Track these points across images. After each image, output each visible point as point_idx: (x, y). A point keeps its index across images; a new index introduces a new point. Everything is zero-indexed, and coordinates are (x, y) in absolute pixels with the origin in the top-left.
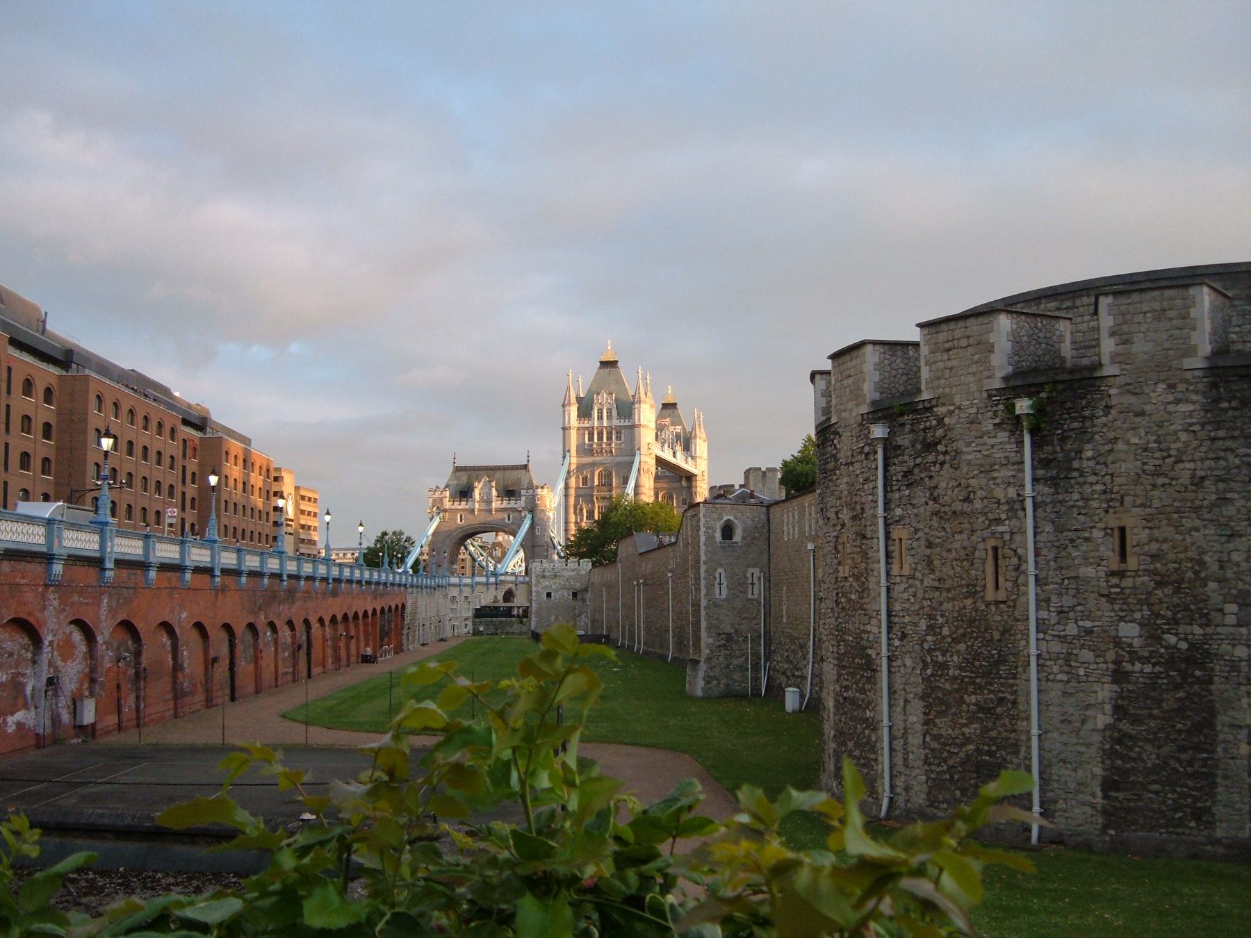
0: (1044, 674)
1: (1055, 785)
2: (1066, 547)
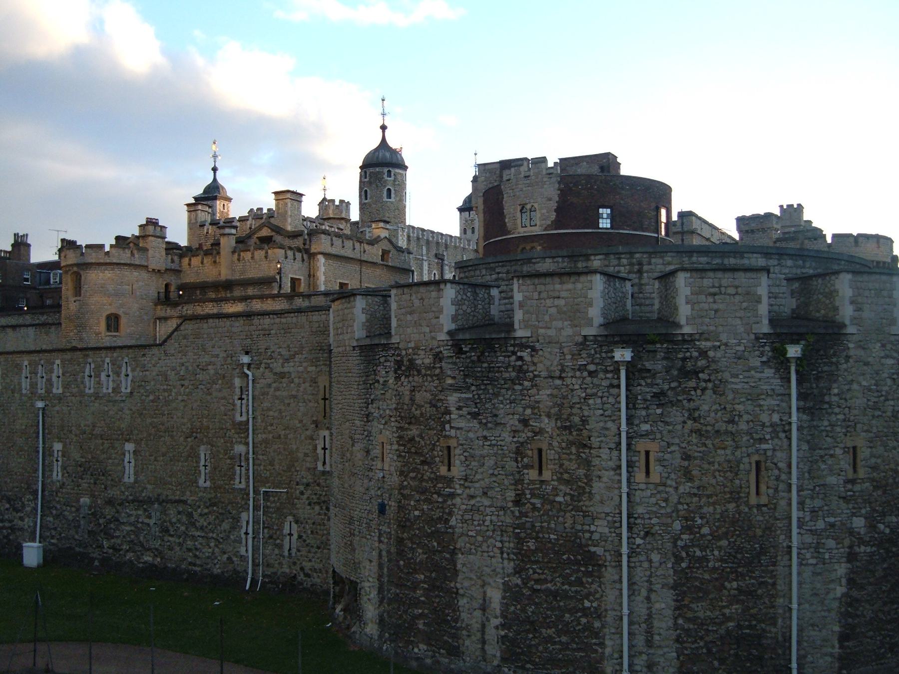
1: (805, 644)
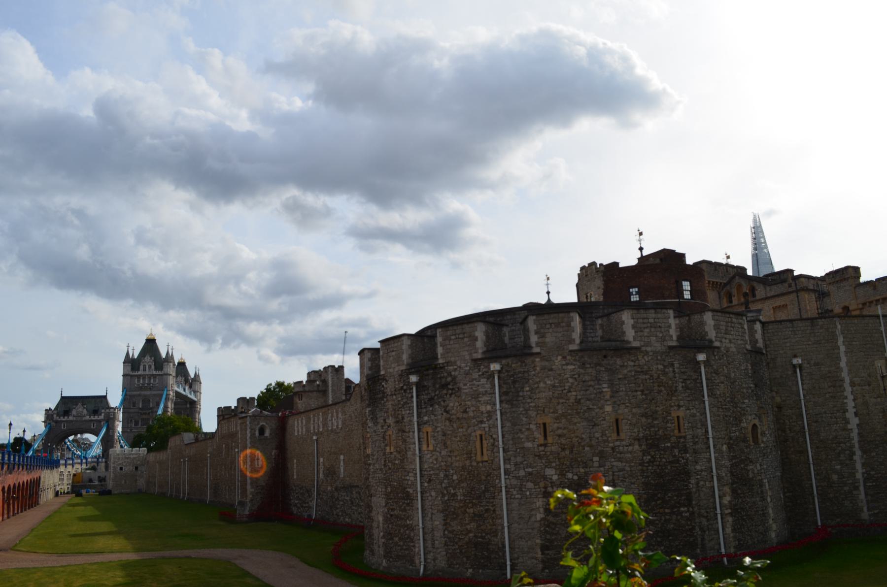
0: (509, 496)
2: (518, 433)
